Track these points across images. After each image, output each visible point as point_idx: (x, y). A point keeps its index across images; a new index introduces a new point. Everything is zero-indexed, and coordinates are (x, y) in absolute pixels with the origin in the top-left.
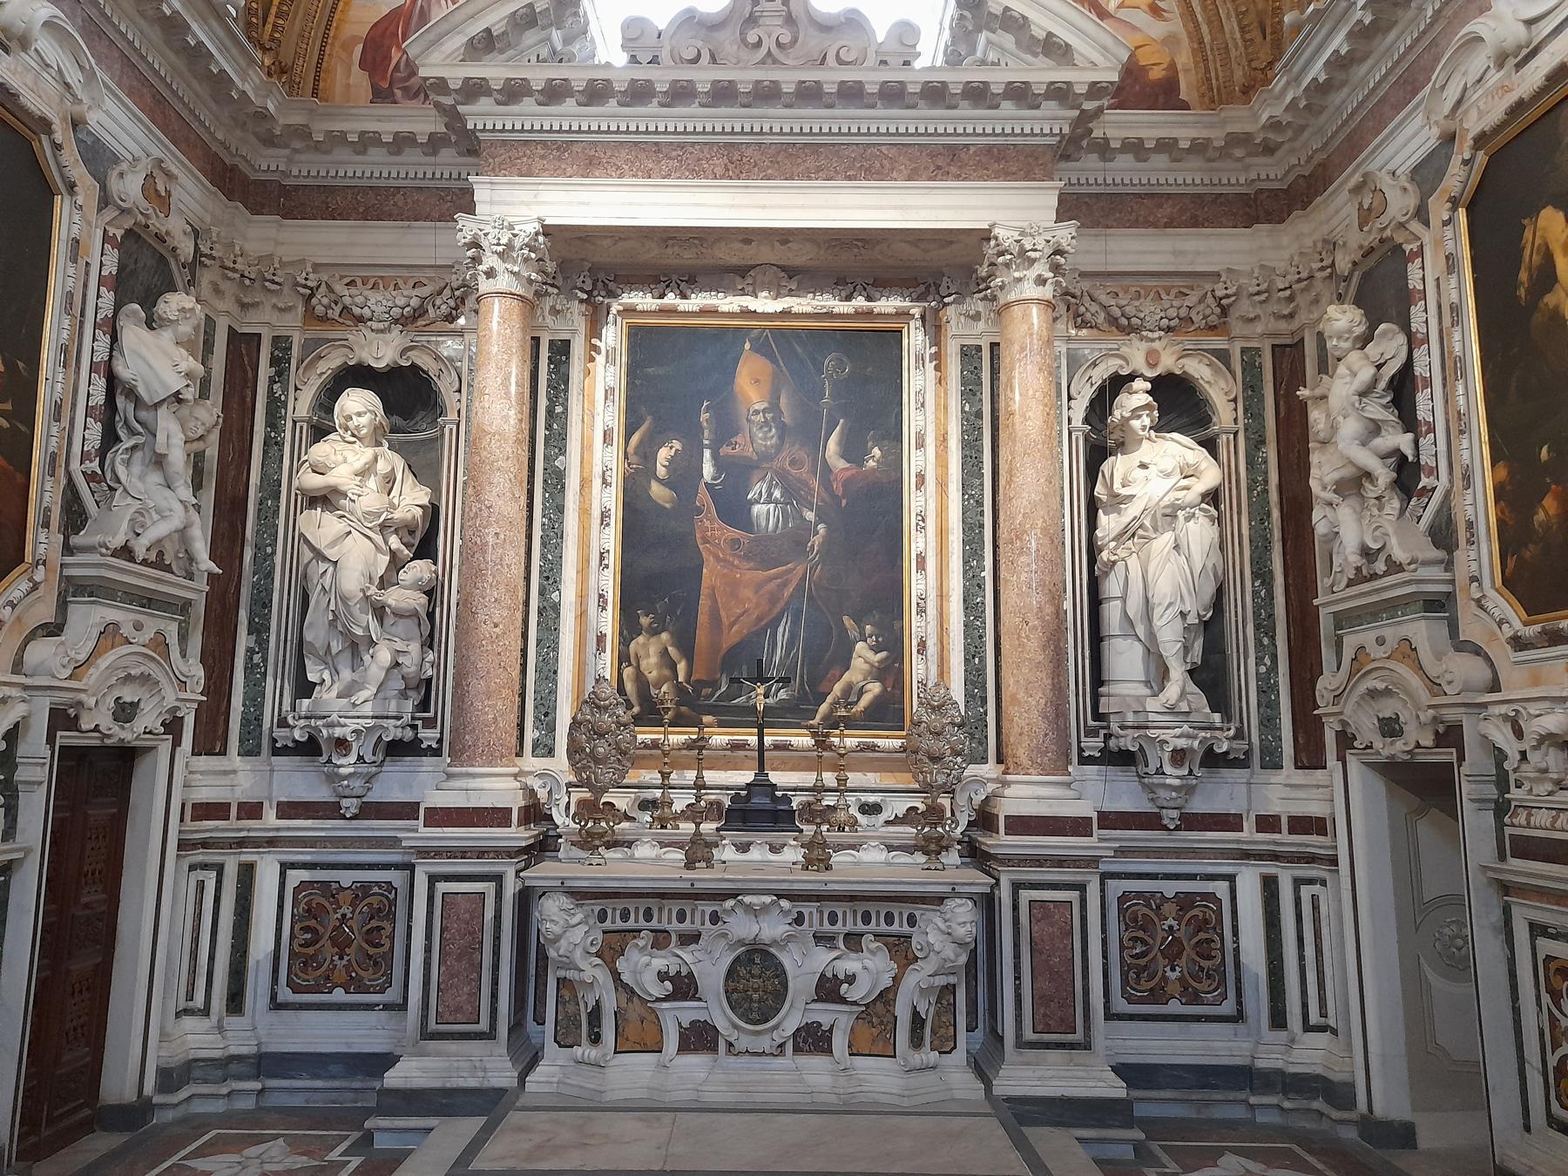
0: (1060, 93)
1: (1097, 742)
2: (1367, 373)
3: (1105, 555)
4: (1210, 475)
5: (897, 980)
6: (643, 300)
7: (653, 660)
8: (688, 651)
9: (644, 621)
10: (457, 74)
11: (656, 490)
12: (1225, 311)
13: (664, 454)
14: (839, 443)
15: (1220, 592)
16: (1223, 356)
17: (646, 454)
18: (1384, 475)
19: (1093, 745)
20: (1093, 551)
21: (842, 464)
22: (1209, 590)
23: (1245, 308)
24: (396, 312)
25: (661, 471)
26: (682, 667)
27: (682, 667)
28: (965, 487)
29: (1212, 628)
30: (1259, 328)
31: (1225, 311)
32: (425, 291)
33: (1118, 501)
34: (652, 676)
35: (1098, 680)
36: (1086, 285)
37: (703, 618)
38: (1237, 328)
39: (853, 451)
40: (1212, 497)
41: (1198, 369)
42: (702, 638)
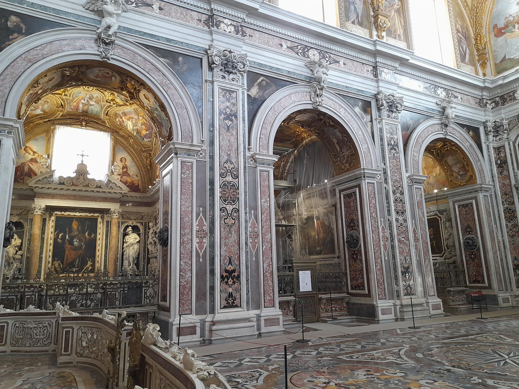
0: (121, 193)
1: (121, 274)
2: (152, 231)
3: (124, 249)
4: (138, 239)
5: (91, 304)
6: (59, 213)
7: (57, 264)
8: (62, 263)
9: (56, 259)
10: (34, 186)
11: (59, 240)
12: (143, 217)
13: (60, 235)
14: (88, 233)
15: (139, 254)
16: (142, 223)
17: (58, 235)
18: (153, 243)
19: (121, 274)
20: (123, 248)
21: (88, 237)
22: (137, 253)
23: (145, 217)
24: (17, 214)
25: (60, 237)
26: (61, 266)
27: (61, 266)
28: (106, 240)
29: (138, 258)
30: (147, 220)
31: (143, 217)
32: (23, 210)
33: (126, 242)
34: (57, 267)
35: (122, 265)
36: (125, 213)
37: (65, 258)
38: (144, 220)
39: (90, 235)
40: (139, 242)
41: (138, 225)
42: (65, 261)
